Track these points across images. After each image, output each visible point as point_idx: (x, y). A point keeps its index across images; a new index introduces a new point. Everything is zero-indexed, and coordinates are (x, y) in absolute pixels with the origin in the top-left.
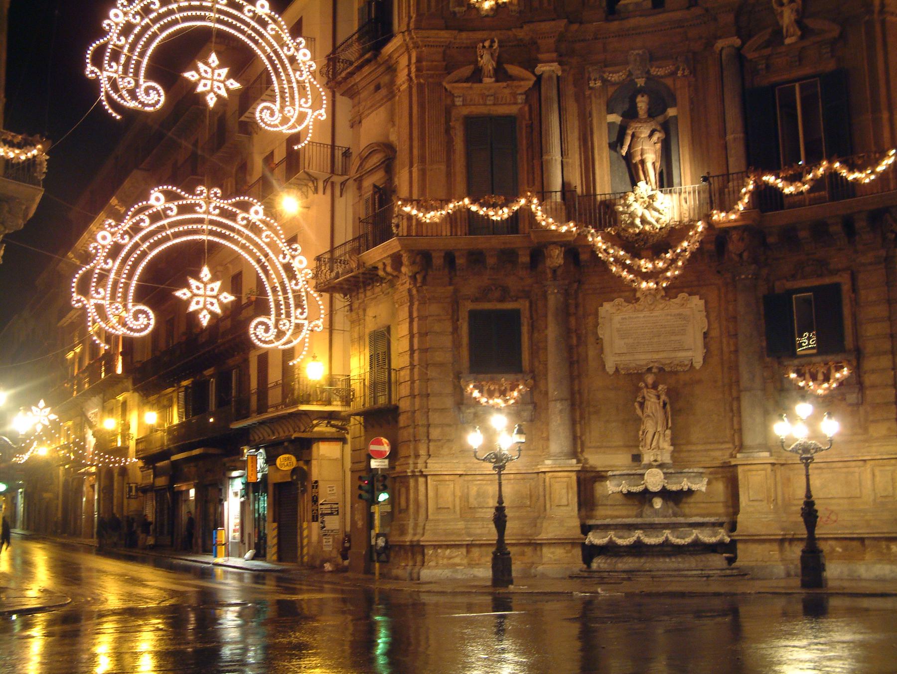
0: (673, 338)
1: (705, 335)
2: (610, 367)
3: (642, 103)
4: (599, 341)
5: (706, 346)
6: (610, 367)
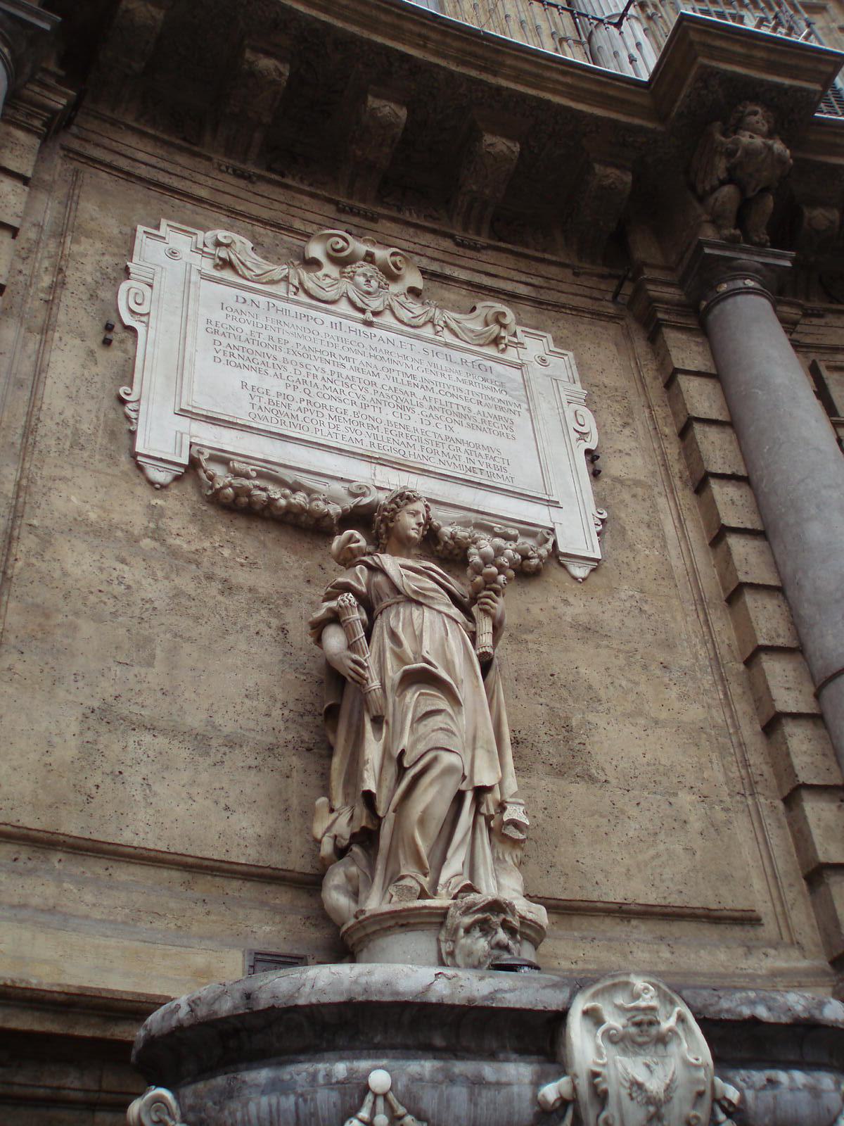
0: (462, 432)
1: (592, 456)
2: (162, 436)
4: (114, 333)
5: (601, 501)
6: (162, 436)
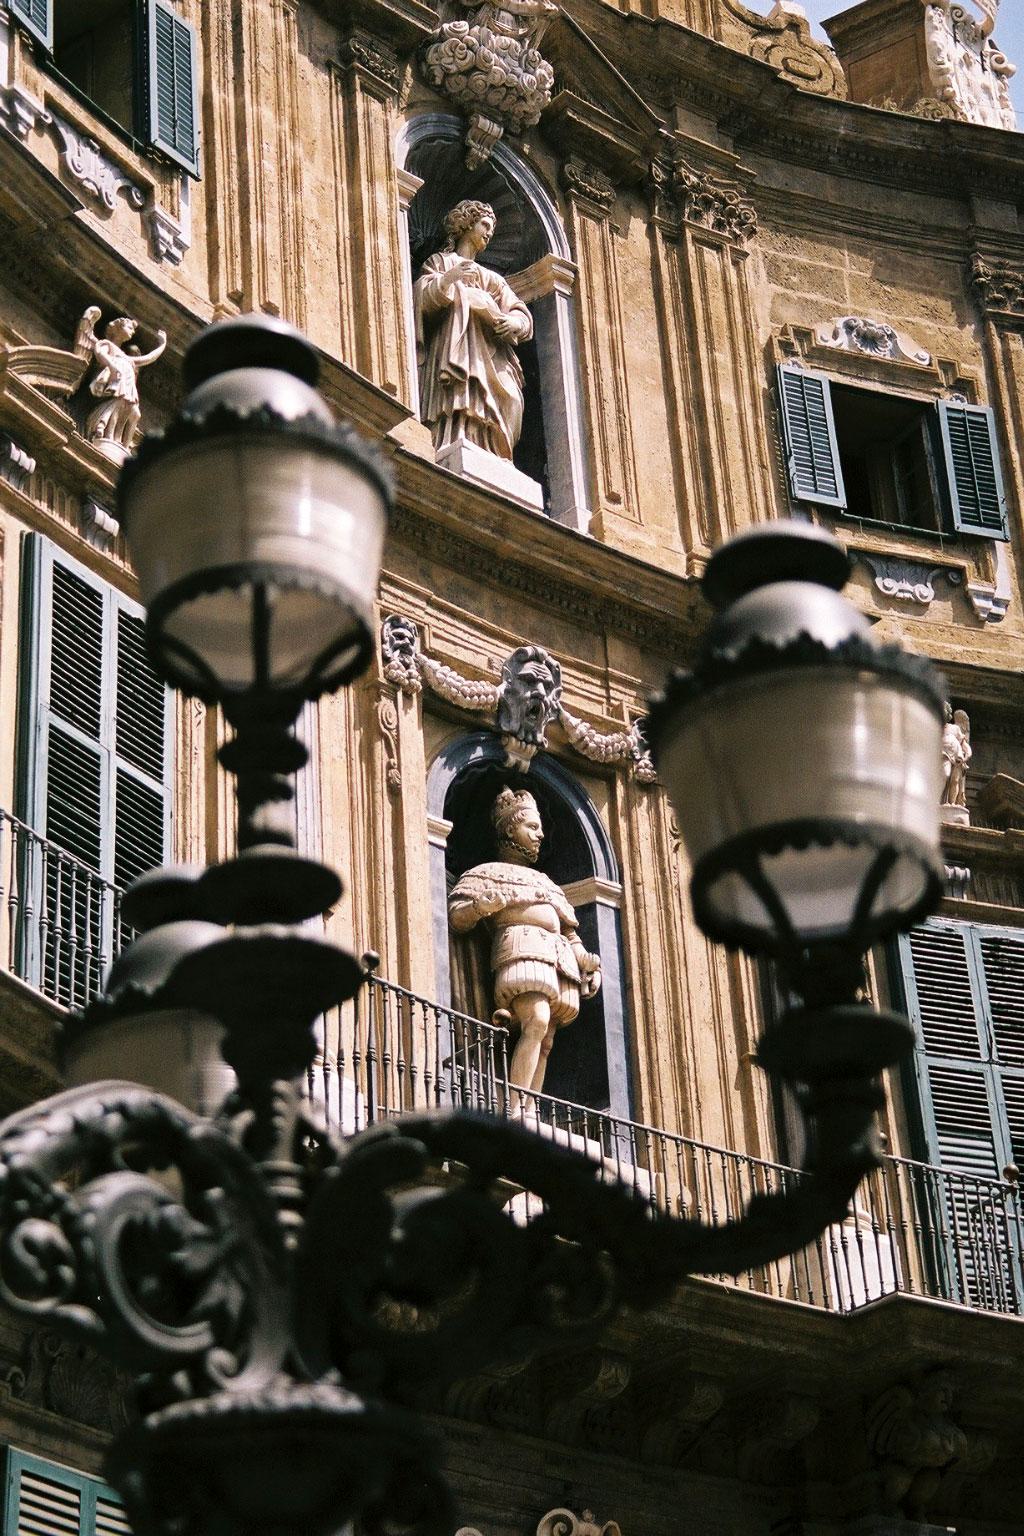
3: (527, 814)
